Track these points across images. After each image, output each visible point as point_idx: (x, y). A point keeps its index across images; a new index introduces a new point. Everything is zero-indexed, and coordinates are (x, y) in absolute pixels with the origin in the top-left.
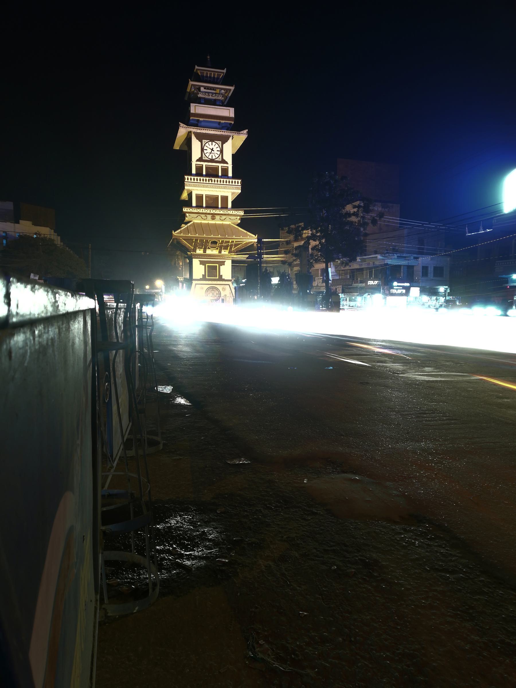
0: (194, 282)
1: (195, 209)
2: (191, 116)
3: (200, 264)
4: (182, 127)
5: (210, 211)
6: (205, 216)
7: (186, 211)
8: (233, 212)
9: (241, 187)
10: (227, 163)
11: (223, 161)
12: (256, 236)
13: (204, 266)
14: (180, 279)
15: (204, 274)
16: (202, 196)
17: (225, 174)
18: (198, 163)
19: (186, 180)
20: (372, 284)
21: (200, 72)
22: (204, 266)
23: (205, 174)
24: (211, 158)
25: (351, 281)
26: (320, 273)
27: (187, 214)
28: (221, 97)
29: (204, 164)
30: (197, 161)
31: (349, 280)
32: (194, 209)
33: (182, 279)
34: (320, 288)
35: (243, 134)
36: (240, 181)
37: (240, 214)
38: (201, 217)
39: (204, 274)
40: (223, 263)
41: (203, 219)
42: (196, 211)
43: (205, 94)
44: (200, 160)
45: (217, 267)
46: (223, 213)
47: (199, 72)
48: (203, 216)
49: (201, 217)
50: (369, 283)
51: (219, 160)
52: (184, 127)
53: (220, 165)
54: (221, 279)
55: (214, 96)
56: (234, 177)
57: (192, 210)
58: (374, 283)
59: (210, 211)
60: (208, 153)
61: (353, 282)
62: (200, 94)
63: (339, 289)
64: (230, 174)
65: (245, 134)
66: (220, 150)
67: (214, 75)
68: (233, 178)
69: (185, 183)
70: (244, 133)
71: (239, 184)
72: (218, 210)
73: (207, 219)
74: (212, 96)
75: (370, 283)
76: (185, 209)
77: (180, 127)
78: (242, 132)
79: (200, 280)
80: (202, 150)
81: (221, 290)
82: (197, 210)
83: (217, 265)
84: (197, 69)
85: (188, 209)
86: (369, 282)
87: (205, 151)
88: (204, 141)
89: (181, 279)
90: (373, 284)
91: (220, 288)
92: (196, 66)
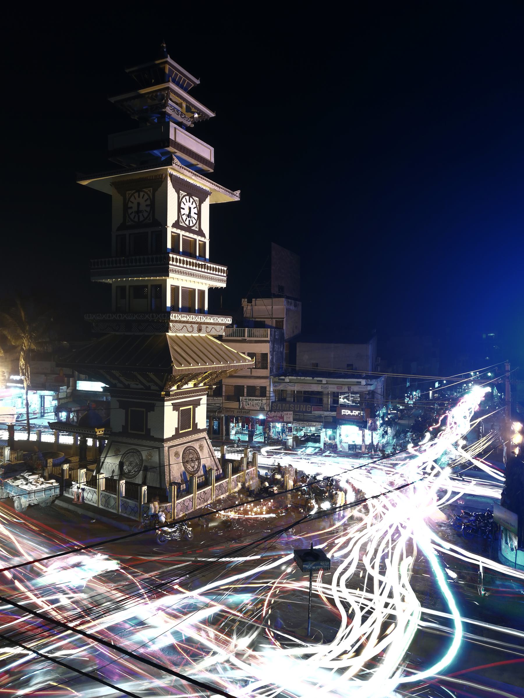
0: (166, 445)
1: (185, 315)
2: (170, 145)
3: (173, 410)
4: (176, 165)
5: (201, 318)
6: (191, 326)
7: (174, 319)
8: (222, 320)
9: (226, 278)
10: (203, 235)
11: (200, 233)
12: (252, 358)
13: (177, 412)
14: (98, 432)
15: (177, 427)
16: (178, 287)
17: (202, 256)
18: (175, 230)
19: (171, 262)
20: (349, 415)
21: (169, 68)
22: (177, 412)
23: (170, 248)
24: (188, 225)
25: (309, 407)
26: (245, 390)
27: (171, 324)
28: (191, 122)
29: (182, 233)
30: (174, 226)
31: (305, 406)
32: (183, 315)
33: (101, 433)
34: (249, 412)
35: (236, 196)
36: (225, 269)
37: (229, 323)
38: (187, 328)
39: (177, 427)
40: (197, 403)
41: (188, 330)
42: (185, 319)
43: (174, 110)
44: (176, 225)
45: (191, 410)
46: (213, 322)
47: (167, 67)
48: (188, 325)
49: (187, 328)
50: (343, 412)
51: (196, 229)
52: (178, 166)
53: (198, 238)
54: (196, 430)
55: (183, 117)
56: (211, 260)
57: (181, 317)
58: (354, 414)
59: (201, 318)
60: (185, 215)
61: (311, 408)
62: (169, 107)
63: (288, 416)
64: (207, 256)
65: (238, 197)
66: (197, 213)
67: (184, 81)
68: (184, 255)
69: (170, 266)
70: (237, 195)
71: (225, 275)
72: (208, 317)
73: (192, 331)
74: (181, 117)
75: (344, 413)
76: (172, 316)
77: (174, 164)
78: (235, 193)
79: (174, 438)
80: (179, 208)
81: (198, 450)
82: (187, 318)
83: (191, 407)
84: (167, 62)
85: (176, 315)
86: (343, 411)
87: (183, 212)
88: (182, 193)
89: (100, 432)
90: (351, 414)
91: (196, 446)
92: (169, 56)
